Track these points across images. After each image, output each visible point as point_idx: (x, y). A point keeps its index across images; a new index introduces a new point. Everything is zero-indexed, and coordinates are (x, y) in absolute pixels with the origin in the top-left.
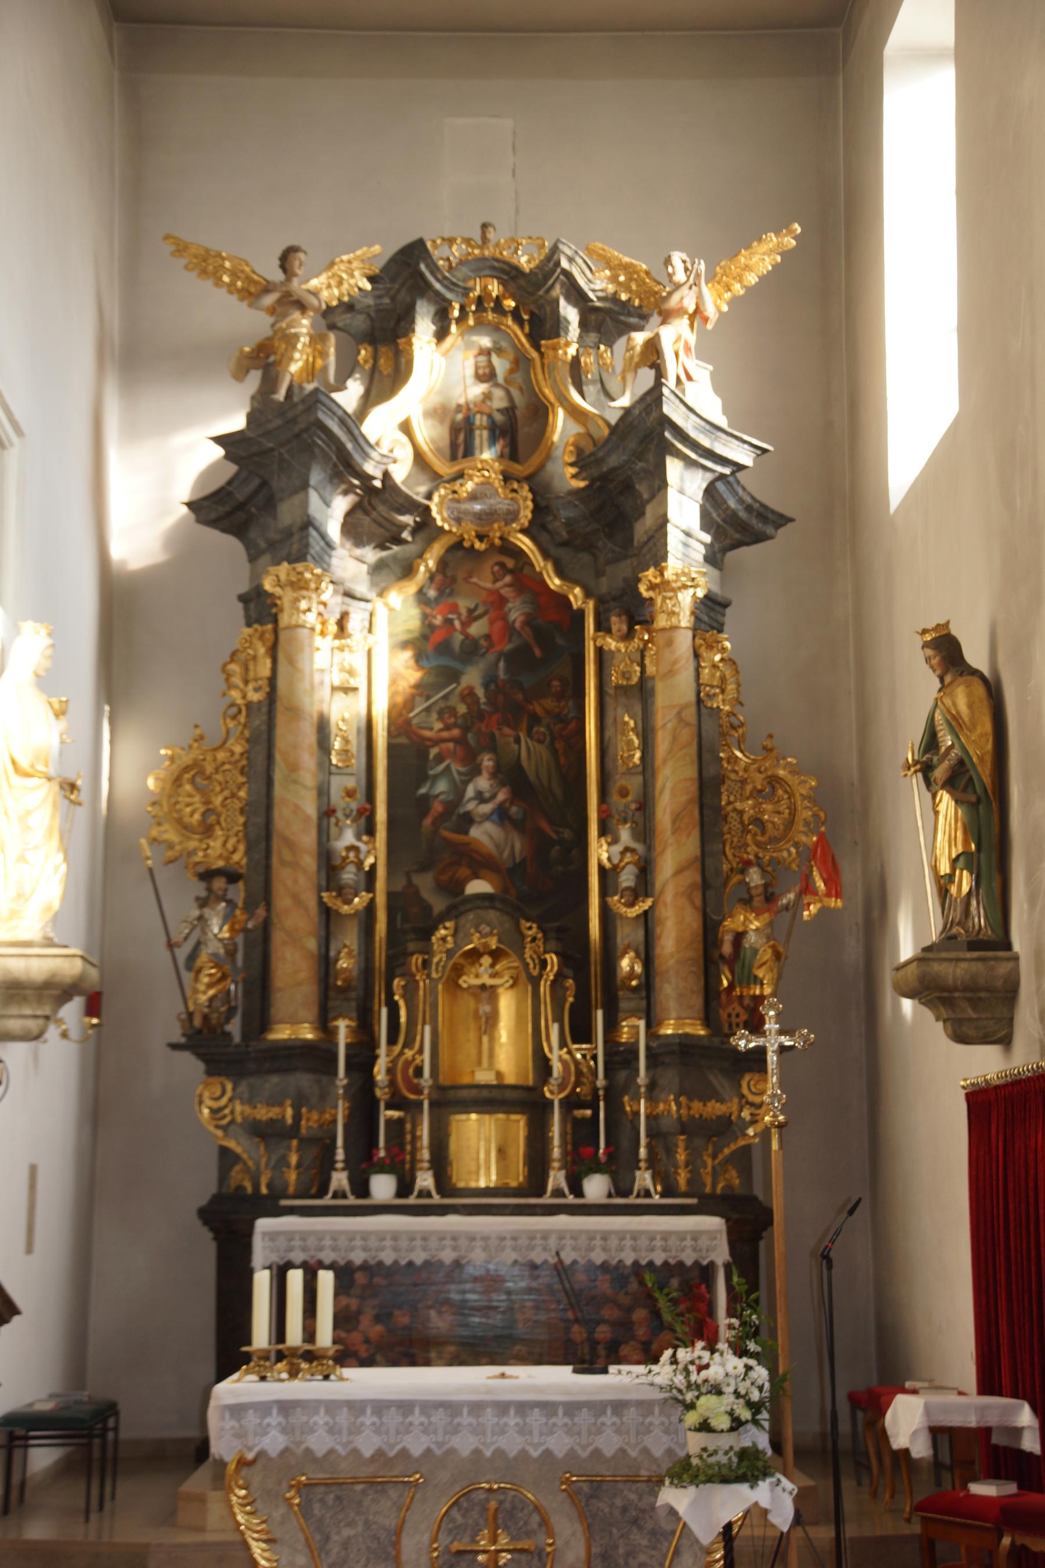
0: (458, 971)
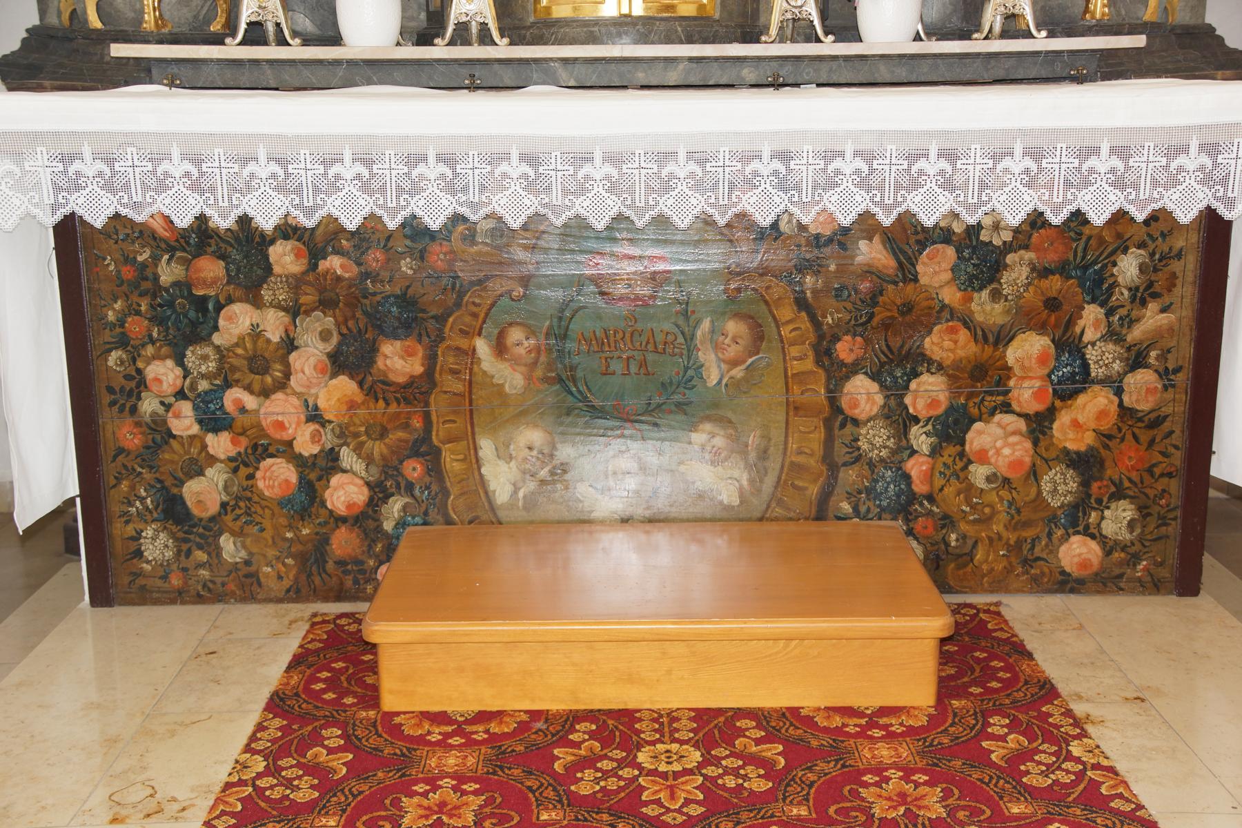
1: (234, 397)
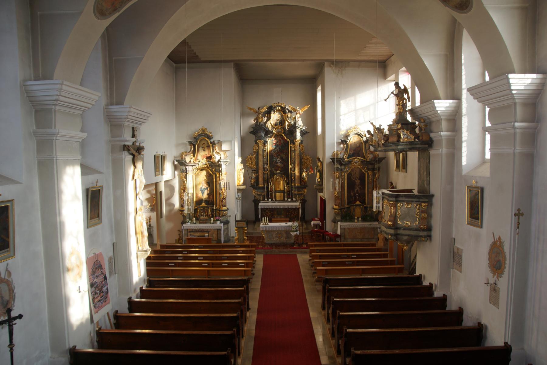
0: (277, 179)
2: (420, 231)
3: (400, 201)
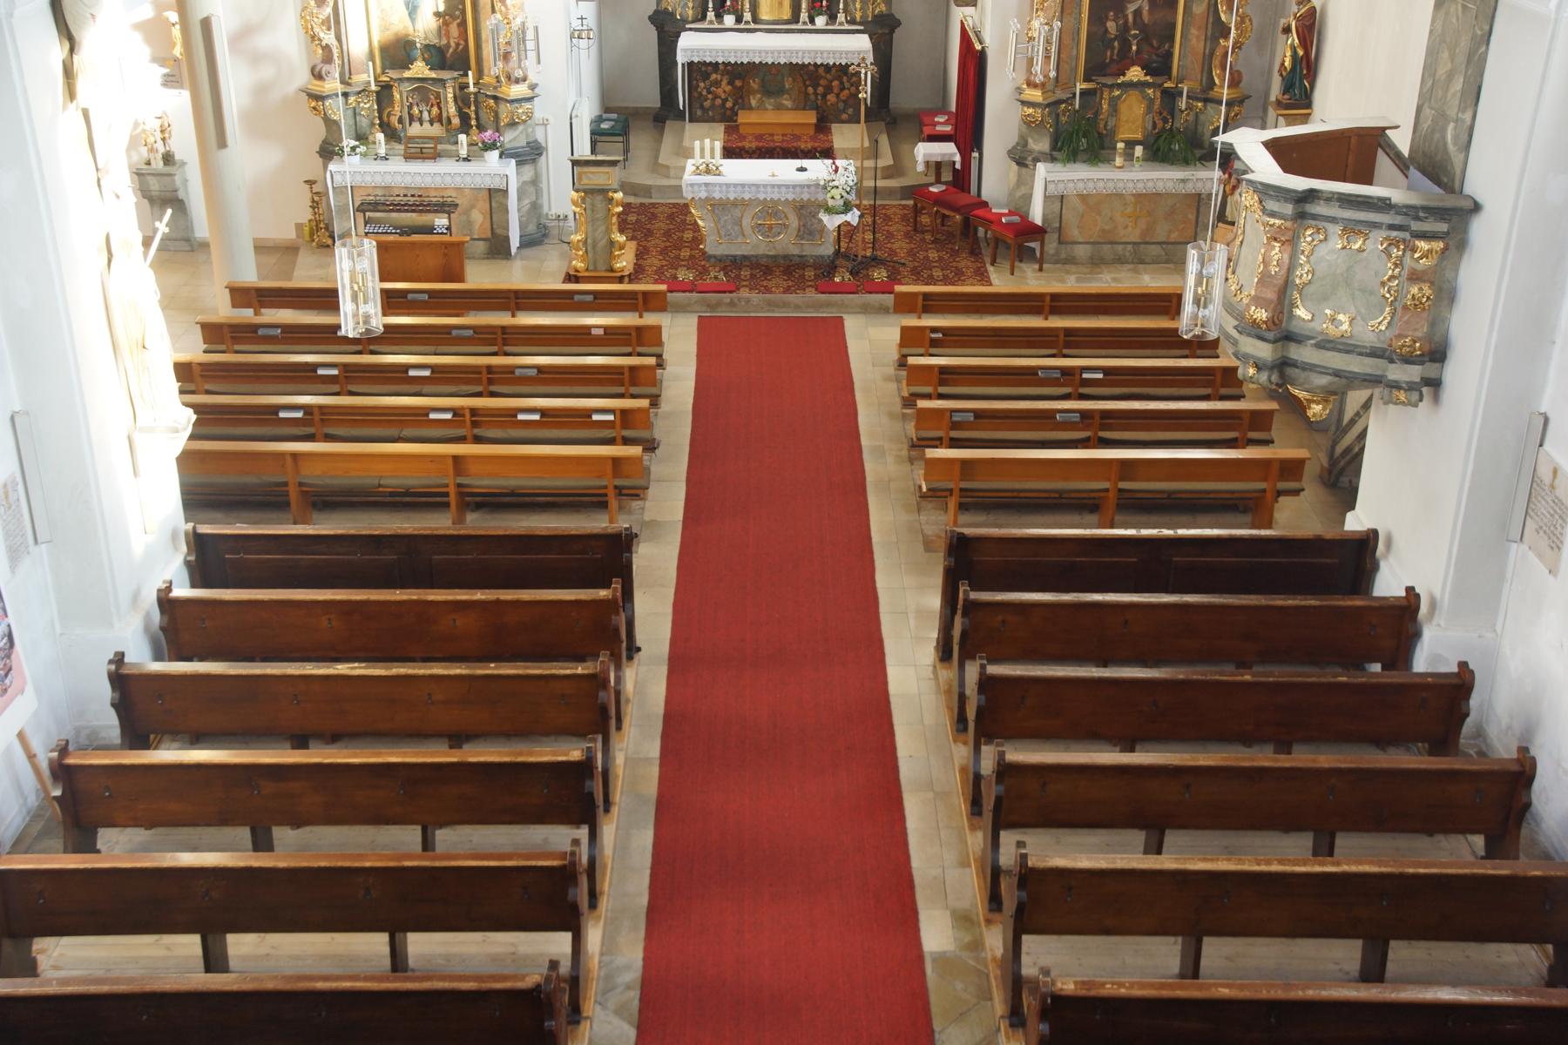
1: (713, 89)
2: (1392, 361)
3: (1315, 217)
